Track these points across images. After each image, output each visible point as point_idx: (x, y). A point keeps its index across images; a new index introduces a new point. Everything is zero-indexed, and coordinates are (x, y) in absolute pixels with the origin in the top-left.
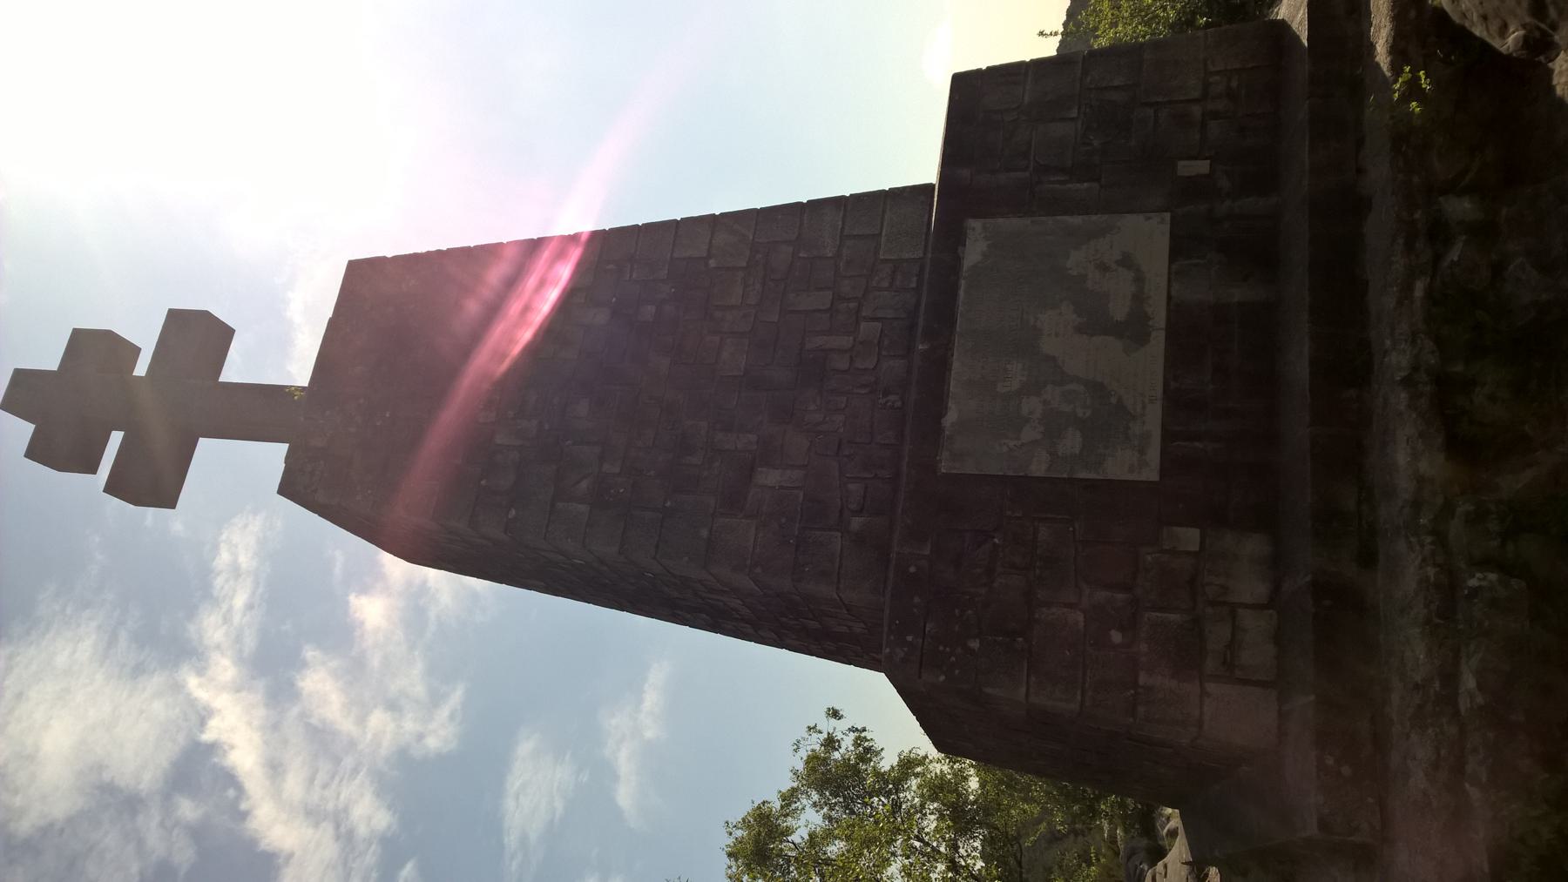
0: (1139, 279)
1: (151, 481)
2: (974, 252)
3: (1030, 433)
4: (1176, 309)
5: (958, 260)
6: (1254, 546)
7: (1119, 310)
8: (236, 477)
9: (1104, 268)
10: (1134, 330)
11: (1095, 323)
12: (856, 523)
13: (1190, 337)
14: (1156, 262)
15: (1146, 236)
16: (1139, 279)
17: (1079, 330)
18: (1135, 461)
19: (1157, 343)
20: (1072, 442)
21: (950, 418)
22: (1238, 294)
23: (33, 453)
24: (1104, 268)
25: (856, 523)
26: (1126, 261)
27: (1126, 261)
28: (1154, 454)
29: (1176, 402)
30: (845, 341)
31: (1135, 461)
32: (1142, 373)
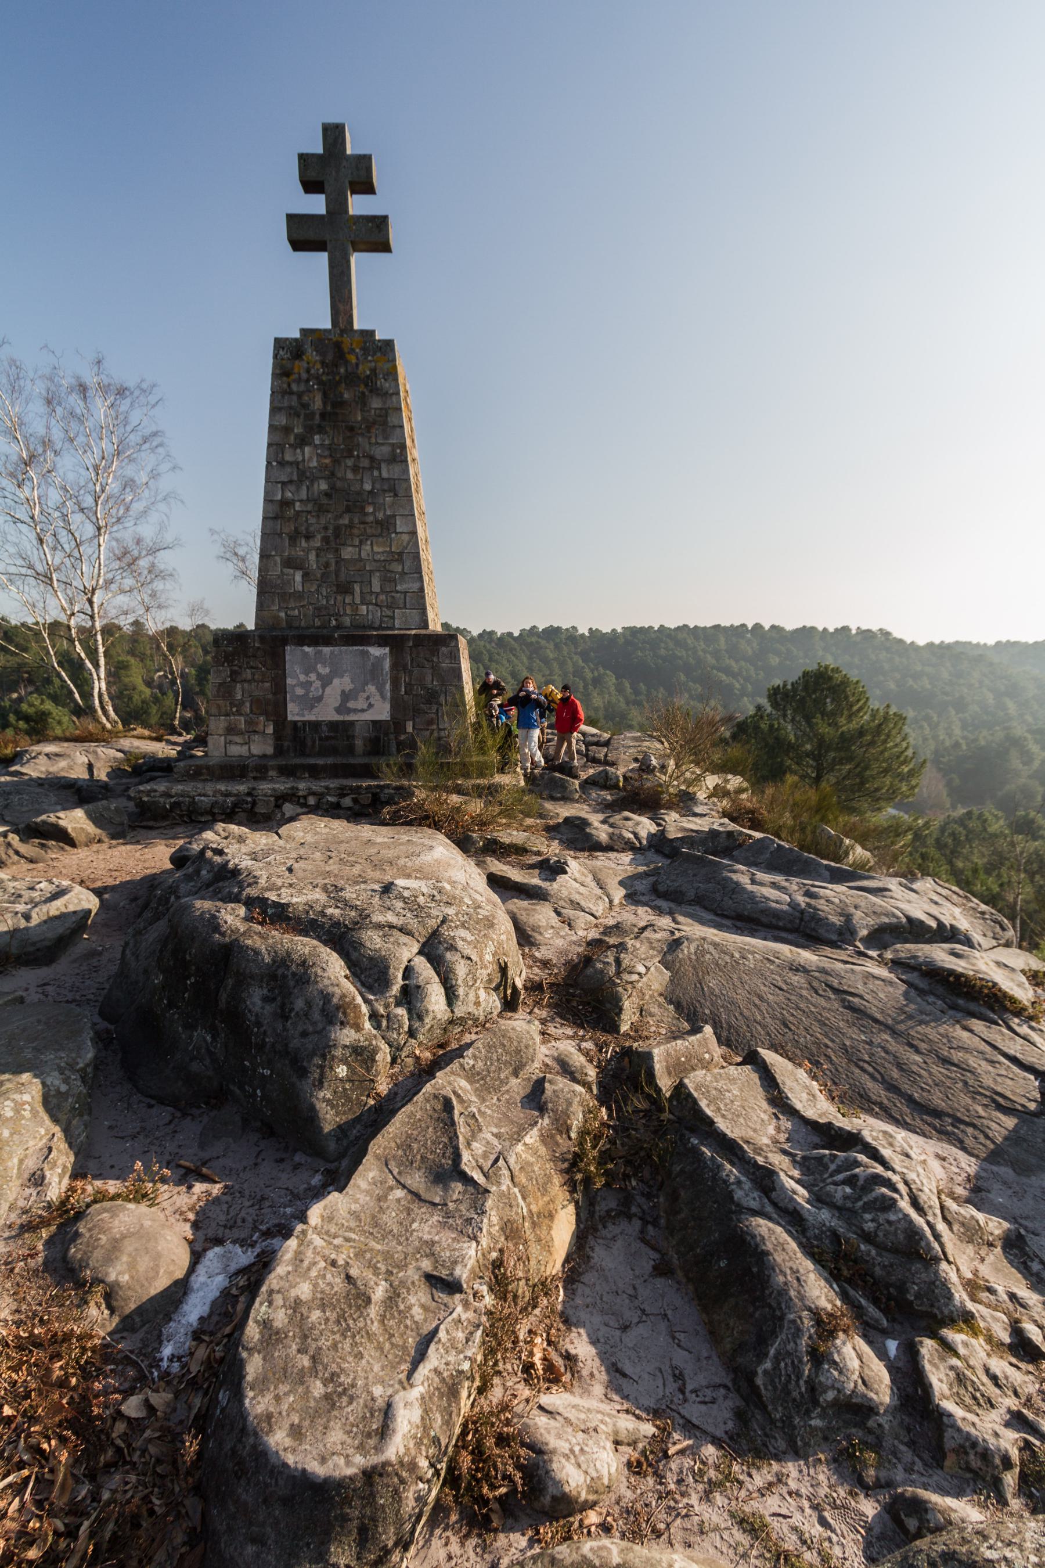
0: (363, 711)
1: (304, 235)
2: (375, 651)
3: (302, 678)
4: (352, 723)
5: (369, 644)
6: (270, 750)
7: (351, 704)
8: (297, 297)
9: (368, 698)
10: (341, 709)
11: (346, 696)
12: (282, 615)
13: (341, 729)
14: (368, 716)
15: (382, 712)
16: (363, 711)
17: (343, 692)
18: (294, 713)
19: (340, 718)
20: (299, 691)
21: (306, 649)
22: (359, 743)
23: (303, 158)
24: (368, 698)
25: (282, 615)
26: (370, 706)
27: (370, 706)
28: (297, 718)
29: (316, 725)
30: (358, 600)
31: (294, 713)
32: (327, 713)
